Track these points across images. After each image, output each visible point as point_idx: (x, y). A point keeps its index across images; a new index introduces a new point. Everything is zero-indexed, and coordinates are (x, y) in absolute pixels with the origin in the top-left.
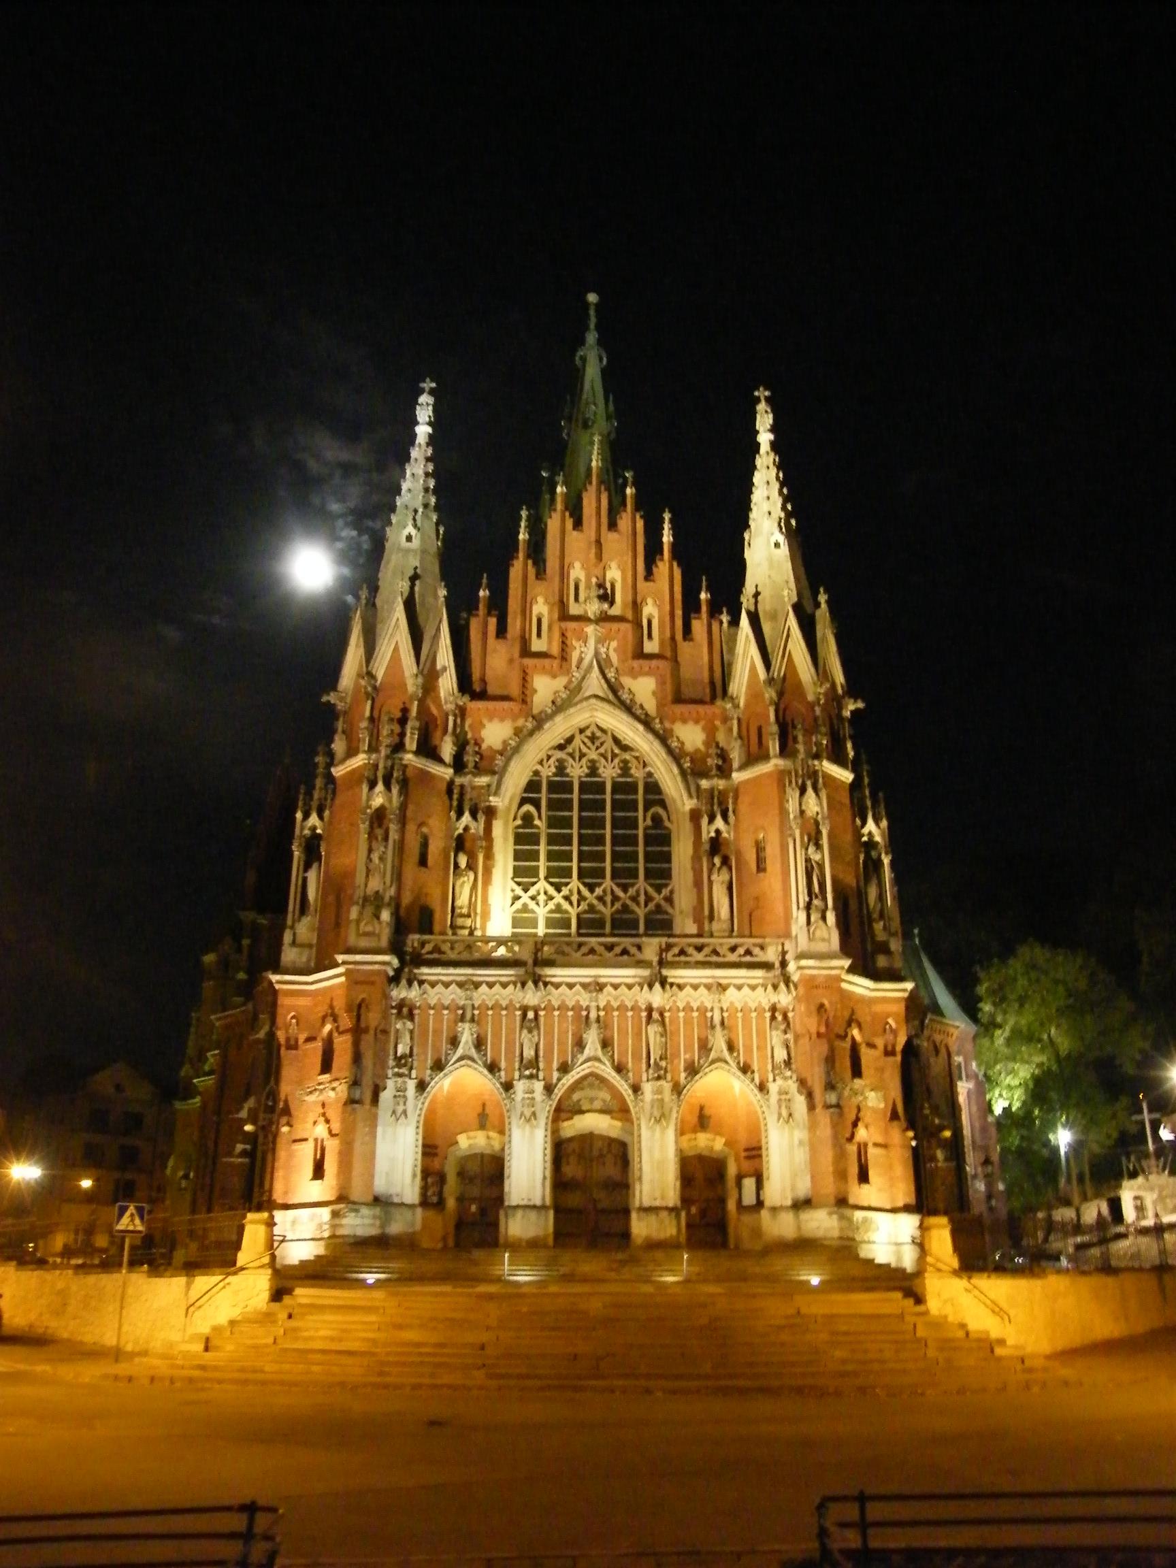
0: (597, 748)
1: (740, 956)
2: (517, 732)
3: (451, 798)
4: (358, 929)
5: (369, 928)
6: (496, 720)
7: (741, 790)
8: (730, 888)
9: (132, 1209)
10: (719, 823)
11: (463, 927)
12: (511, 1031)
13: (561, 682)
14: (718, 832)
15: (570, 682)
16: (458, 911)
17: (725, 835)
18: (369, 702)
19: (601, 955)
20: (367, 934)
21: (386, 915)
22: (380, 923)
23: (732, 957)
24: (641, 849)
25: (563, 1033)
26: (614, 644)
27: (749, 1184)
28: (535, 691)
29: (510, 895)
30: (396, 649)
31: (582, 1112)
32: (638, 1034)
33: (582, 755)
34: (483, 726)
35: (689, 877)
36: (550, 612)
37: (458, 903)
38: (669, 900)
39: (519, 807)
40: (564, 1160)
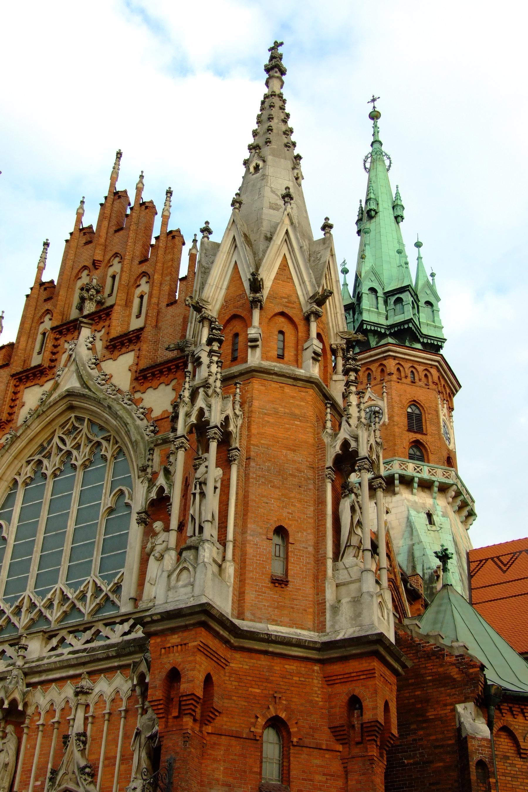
1: (125, 634)
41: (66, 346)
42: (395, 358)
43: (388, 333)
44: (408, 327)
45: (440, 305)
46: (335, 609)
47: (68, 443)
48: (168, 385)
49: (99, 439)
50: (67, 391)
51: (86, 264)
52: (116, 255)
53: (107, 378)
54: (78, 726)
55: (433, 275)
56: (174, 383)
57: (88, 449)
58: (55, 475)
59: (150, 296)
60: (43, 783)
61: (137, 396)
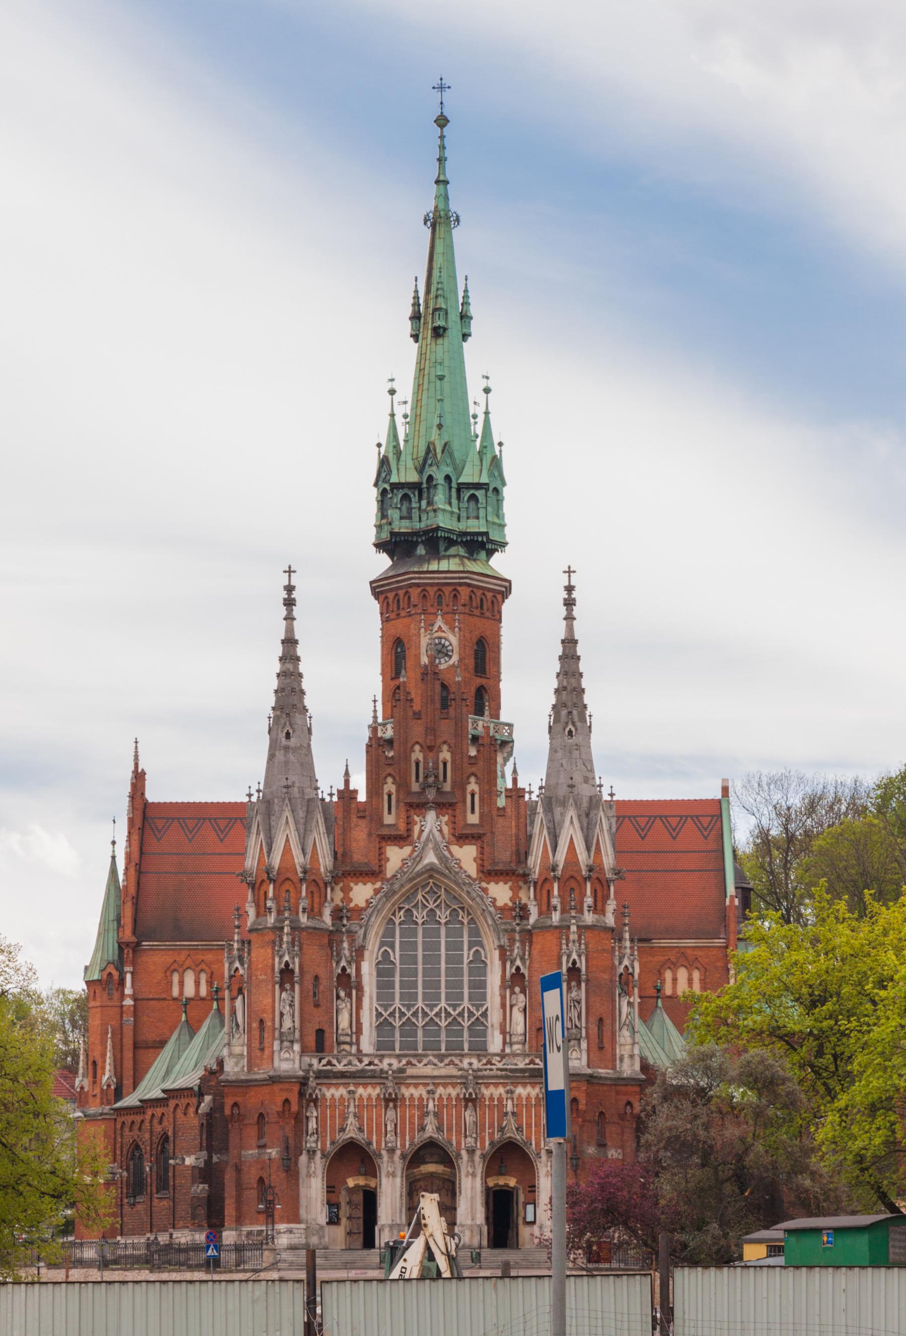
0: (435, 901)
2: (377, 891)
3: (331, 949)
4: (279, 1056)
5: (287, 1055)
6: (360, 884)
7: (534, 940)
8: (525, 1010)
9: (212, 1247)
10: (518, 963)
11: (344, 1043)
12: (379, 1116)
13: (408, 850)
14: (518, 969)
15: (413, 851)
16: (340, 1031)
17: (522, 971)
18: (271, 886)
19: (435, 1065)
20: (287, 1059)
21: (297, 1047)
22: (294, 1052)
23: (521, 1065)
24: (466, 979)
25: (412, 1117)
26: (446, 818)
27: (530, 1208)
28: (388, 860)
29: (374, 1013)
30: (287, 840)
31: (425, 1163)
32: (459, 1117)
33: (425, 906)
34: (351, 889)
35: (498, 1000)
36: (398, 791)
37: (341, 1027)
38: (485, 1014)
39: (379, 949)
40: (415, 1193)
41: (416, 818)
42: (469, 585)
43: (459, 540)
44: (482, 541)
45: (506, 492)
46: (622, 1060)
47: (431, 903)
48: (506, 883)
49: (456, 907)
50: (427, 865)
51: (419, 740)
52: (445, 742)
53: (458, 862)
54: (510, 1108)
55: (500, 444)
56: (510, 884)
57: (448, 912)
58: (423, 924)
59: (482, 800)
60: (493, 1132)
61: (484, 885)
